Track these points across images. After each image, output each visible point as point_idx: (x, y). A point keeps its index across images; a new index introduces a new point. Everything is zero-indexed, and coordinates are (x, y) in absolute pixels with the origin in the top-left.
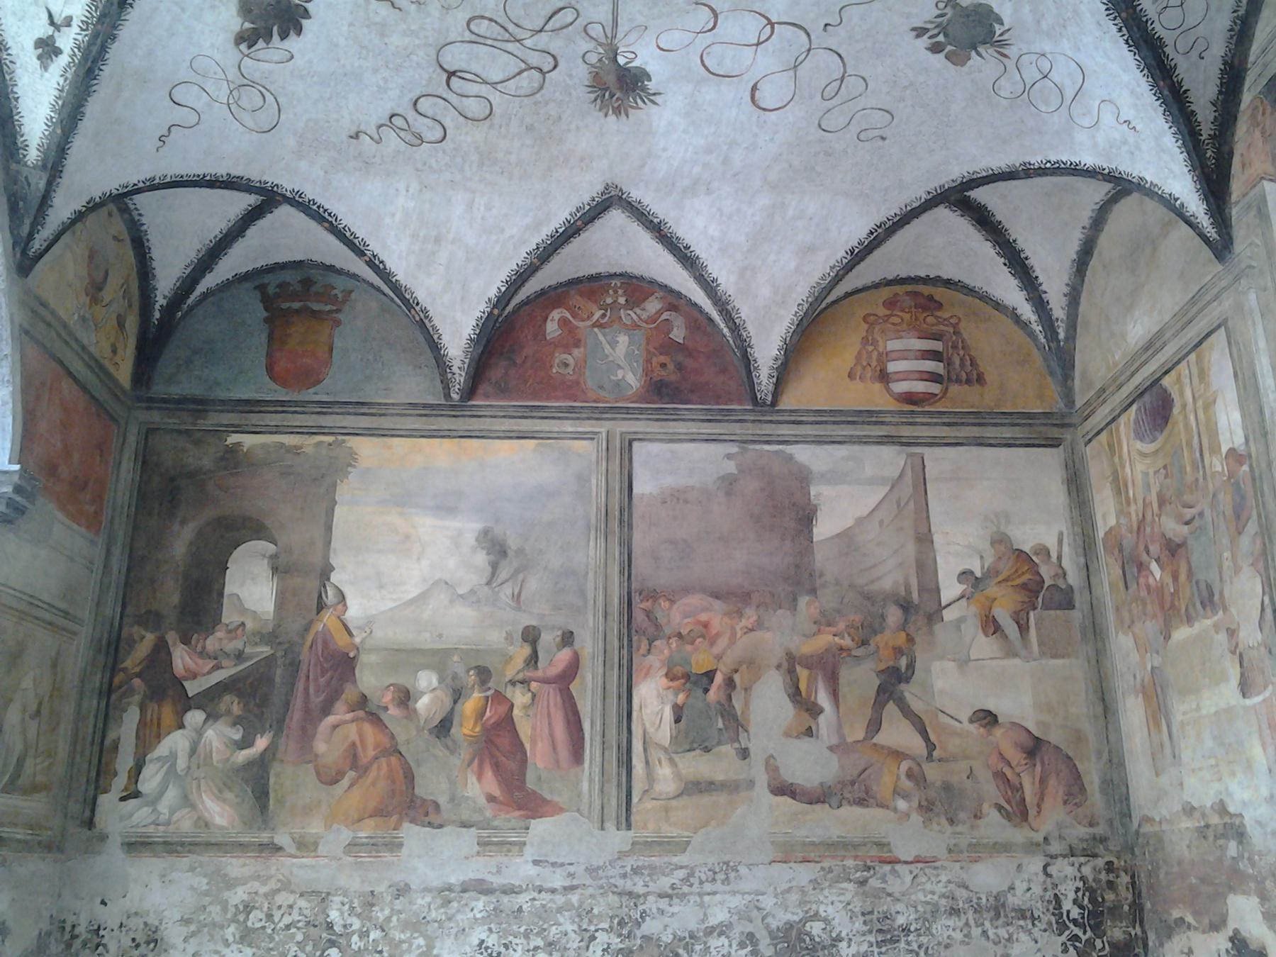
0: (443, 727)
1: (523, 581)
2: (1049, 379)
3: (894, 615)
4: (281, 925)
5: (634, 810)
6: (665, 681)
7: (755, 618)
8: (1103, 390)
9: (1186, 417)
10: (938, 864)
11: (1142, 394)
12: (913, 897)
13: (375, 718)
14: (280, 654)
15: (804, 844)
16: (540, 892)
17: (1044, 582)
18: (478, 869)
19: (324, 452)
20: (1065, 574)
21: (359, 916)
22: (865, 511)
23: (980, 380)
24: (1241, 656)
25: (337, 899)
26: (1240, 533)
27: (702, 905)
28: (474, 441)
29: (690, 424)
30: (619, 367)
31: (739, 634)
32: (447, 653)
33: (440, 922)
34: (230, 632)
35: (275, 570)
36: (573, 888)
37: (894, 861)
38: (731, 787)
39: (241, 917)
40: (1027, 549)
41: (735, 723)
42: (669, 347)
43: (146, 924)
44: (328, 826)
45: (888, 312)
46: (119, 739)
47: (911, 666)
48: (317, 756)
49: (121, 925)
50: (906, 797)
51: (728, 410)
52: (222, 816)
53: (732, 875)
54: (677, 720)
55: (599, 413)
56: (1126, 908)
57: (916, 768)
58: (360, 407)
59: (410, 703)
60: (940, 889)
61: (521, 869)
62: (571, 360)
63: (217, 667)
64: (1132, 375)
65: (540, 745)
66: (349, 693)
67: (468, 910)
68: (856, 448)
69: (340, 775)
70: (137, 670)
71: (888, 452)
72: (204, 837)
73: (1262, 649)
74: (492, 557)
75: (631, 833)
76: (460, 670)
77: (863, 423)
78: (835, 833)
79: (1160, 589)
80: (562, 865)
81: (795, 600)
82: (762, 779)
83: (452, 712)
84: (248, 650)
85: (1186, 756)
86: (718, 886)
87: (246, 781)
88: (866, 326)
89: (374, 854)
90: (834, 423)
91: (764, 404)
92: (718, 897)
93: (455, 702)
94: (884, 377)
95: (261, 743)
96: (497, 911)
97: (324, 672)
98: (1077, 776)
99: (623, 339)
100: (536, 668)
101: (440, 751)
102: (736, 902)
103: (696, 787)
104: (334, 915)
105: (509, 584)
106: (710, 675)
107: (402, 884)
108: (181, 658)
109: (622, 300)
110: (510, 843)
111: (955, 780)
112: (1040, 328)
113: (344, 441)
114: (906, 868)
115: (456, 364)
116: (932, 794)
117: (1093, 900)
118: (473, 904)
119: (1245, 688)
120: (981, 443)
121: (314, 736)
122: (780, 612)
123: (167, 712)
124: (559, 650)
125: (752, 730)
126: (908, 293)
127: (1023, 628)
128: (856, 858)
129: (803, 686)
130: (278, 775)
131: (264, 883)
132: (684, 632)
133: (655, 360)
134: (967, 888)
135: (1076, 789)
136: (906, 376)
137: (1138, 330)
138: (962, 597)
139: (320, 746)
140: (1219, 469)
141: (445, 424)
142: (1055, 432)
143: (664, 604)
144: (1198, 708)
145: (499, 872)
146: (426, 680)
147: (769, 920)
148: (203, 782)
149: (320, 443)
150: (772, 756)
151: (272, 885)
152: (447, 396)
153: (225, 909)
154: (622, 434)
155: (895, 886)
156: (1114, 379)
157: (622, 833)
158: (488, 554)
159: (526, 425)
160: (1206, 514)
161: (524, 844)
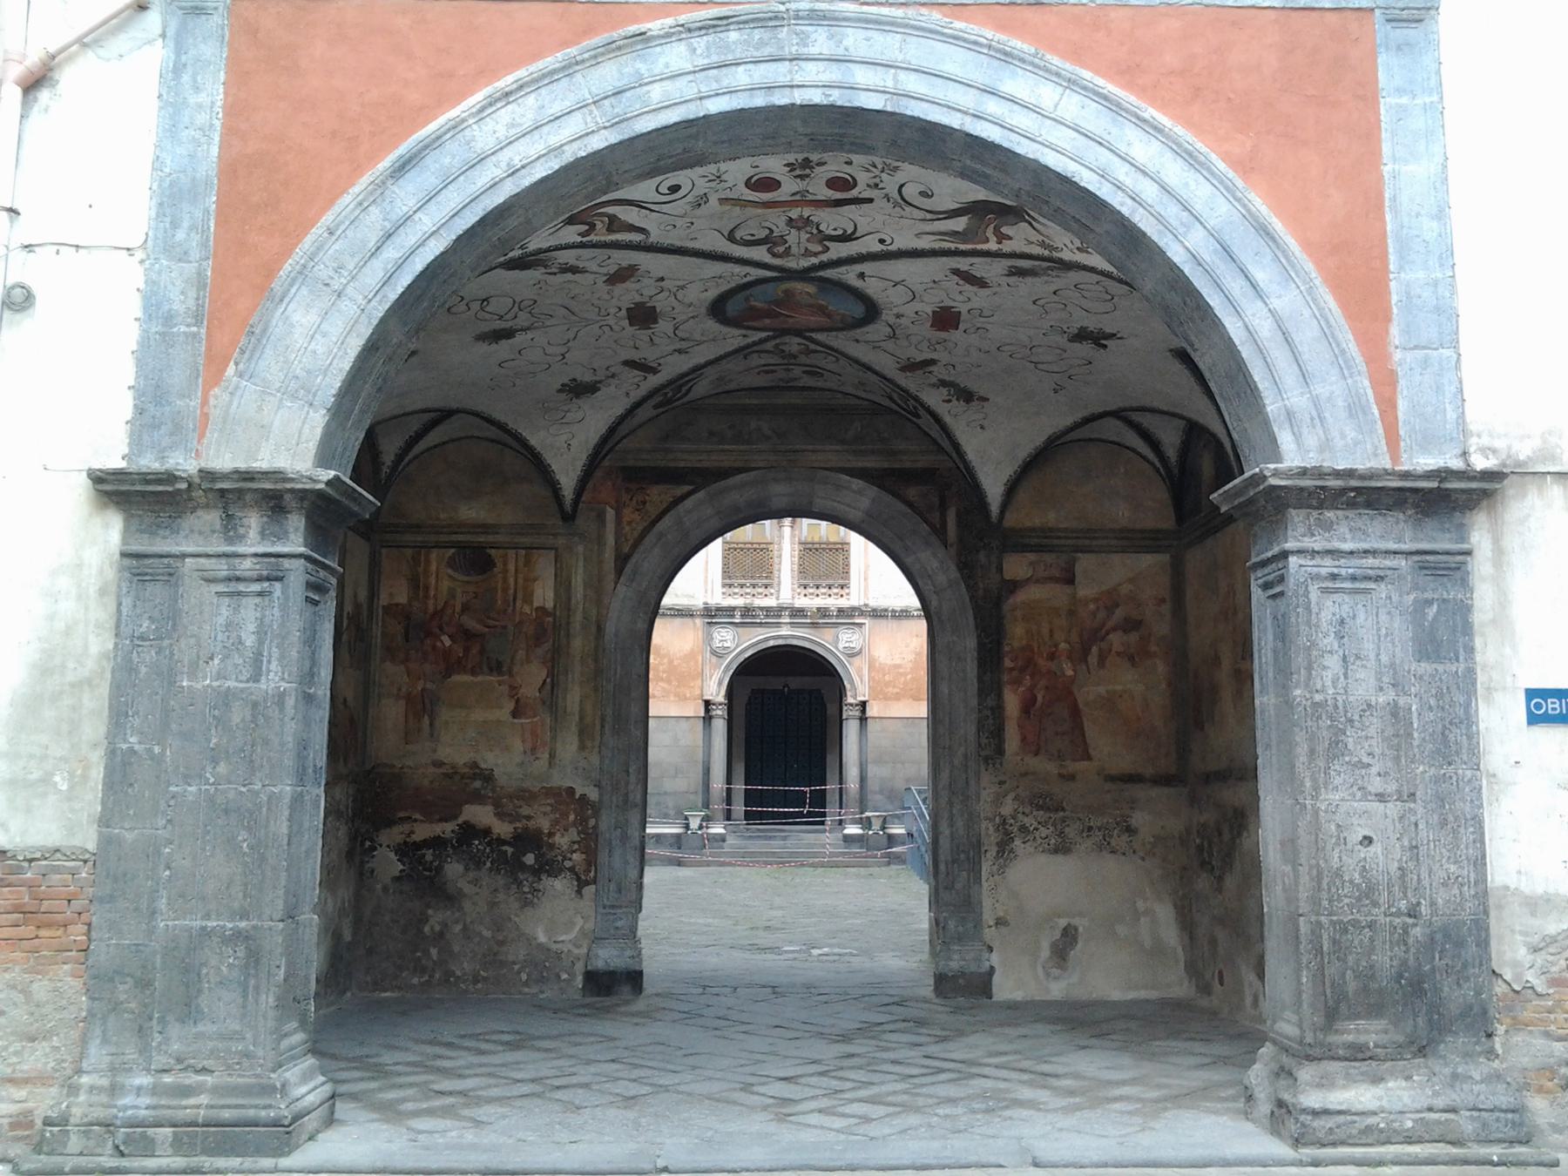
8: (418, 526)
79: (447, 653)
137: (470, 512)
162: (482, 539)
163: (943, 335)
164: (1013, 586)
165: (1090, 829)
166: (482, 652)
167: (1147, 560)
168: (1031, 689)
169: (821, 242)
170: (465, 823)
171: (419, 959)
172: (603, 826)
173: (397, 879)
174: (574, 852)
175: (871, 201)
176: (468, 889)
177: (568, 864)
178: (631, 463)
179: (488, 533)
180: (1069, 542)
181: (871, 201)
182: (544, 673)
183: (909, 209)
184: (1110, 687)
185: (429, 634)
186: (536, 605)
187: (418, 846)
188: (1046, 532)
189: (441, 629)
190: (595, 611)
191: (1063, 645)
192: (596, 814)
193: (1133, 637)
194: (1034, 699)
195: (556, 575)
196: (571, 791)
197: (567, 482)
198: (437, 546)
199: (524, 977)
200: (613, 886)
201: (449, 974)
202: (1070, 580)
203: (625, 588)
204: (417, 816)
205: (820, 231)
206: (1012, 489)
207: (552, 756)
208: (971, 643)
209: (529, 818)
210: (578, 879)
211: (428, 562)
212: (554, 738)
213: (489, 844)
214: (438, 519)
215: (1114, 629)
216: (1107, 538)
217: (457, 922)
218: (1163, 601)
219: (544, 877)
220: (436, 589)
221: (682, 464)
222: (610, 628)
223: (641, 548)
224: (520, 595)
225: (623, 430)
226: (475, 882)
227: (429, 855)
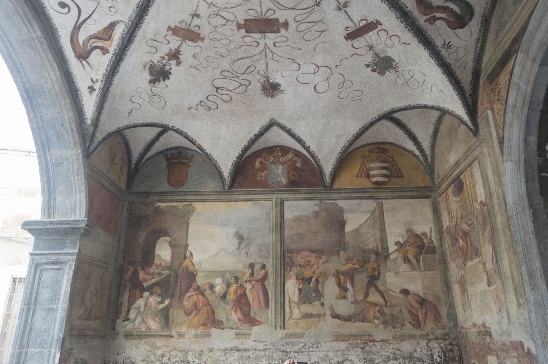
0: (224, 296)
1: (249, 248)
2: (426, 175)
3: (373, 257)
4: (173, 361)
5: (286, 323)
6: (295, 280)
7: (326, 259)
8: (443, 179)
9: (467, 190)
10: (389, 342)
11: (454, 181)
12: (381, 353)
13: (203, 294)
14: (172, 273)
15: (343, 335)
16: (256, 351)
17: (425, 245)
18: (236, 343)
19: (185, 207)
20: (432, 242)
21: (198, 358)
22: (363, 222)
23: (402, 176)
24: (487, 273)
25: (191, 353)
27: (309, 355)
28: (233, 202)
29: (303, 194)
30: (279, 176)
31: (320, 265)
32: (225, 272)
33: (223, 361)
34: (157, 266)
35: (171, 246)
36: (266, 349)
37: (374, 341)
38: (318, 316)
39: (161, 359)
40: (419, 233)
41: (319, 295)
42: (296, 169)
43: (131, 361)
44: (188, 329)
45: (369, 154)
46: (123, 301)
47: (379, 274)
48: (184, 306)
49: (123, 362)
50: (378, 319)
51: (316, 189)
52: (155, 326)
53: (319, 345)
54: (300, 293)
55: (273, 193)
56: (457, 359)
57: (381, 309)
58: (196, 193)
59: (213, 288)
60: (390, 351)
61: (249, 343)
62: (264, 175)
63: (153, 278)
65: (255, 302)
66: (194, 286)
67: (232, 356)
68: (359, 201)
69: (192, 312)
70: (128, 279)
71: (370, 202)
72: (149, 333)
74: (239, 240)
75: (285, 331)
76: (229, 277)
77: (362, 192)
78: (354, 331)
80: (263, 342)
81: (339, 253)
82: (329, 313)
83: (226, 291)
84: (162, 272)
85: (473, 306)
86: (314, 349)
87: (162, 315)
88: (362, 159)
89: (202, 338)
90: (352, 192)
91: (328, 187)
92: (314, 353)
93: (228, 288)
94: (368, 176)
95: (167, 302)
96: (242, 357)
97: (186, 279)
98: (438, 312)
99: (281, 167)
100: (253, 277)
101: (223, 304)
102: (320, 354)
103: (306, 316)
104: (190, 358)
105: (245, 249)
106: (311, 278)
107: (211, 348)
108: (142, 275)
109: (280, 154)
110: (246, 335)
111: (395, 313)
113: (192, 204)
114: (378, 343)
115: (227, 178)
116: (387, 318)
117: (445, 355)
118: (234, 354)
119: (489, 284)
120: (402, 197)
121: (183, 300)
122: (334, 257)
123: (138, 292)
124: (261, 270)
125: (325, 296)
126: (376, 148)
127: (418, 261)
128: (361, 340)
129: (342, 282)
130: (172, 312)
131: (168, 348)
132: (302, 264)
133: (291, 174)
134: (400, 350)
135: (437, 317)
136: (376, 176)
137: (452, 159)
138: (396, 250)
139: (185, 303)
140: (478, 208)
141: (224, 197)
142: (428, 193)
143: (295, 255)
144: (476, 290)
145: (242, 344)
146: (218, 281)
147: (332, 361)
148: (149, 315)
149: (184, 205)
150: (332, 305)
151: (170, 348)
152: (224, 188)
153: (155, 357)
154: (280, 198)
155: (374, 349)
156: (446, 175)
157: (282, 331)
158: (238, 239)
159: (249, 197)
161: (250, 335)
179: (458, 166)
186: (479, 201)
195: (482, 176)
214: (447, 170)
222: (510, 200)
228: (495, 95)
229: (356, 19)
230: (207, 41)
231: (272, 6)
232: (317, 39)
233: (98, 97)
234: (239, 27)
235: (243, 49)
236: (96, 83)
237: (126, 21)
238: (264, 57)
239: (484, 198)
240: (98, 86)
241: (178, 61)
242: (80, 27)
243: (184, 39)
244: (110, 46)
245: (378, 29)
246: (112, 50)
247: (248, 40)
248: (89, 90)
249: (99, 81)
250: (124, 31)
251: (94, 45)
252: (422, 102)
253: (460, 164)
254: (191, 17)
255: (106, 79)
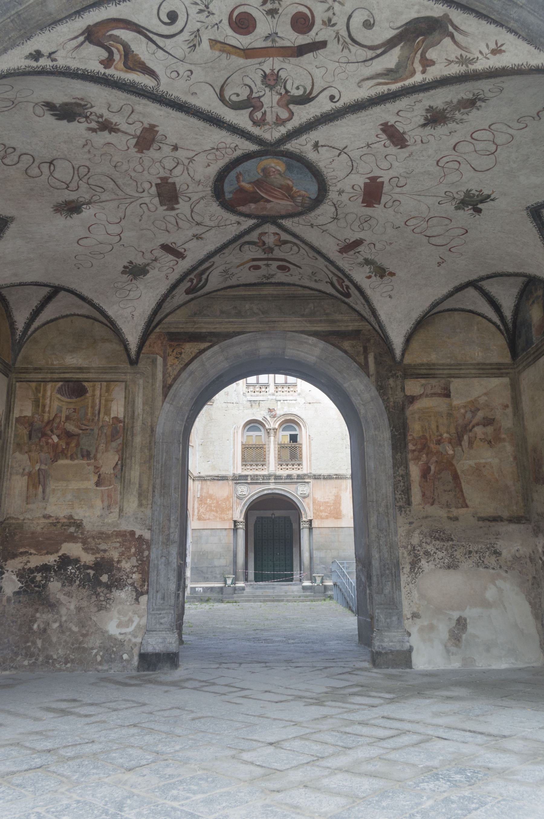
8: (40, 369)
26: (112, 441)
64: (64, 373)
73: (112, 475)
79: (55, 446)
85: (52, 500)
112: (21, 334)
119: (98, 484)
140: (108, 420)
144: (67, 486)
156: (49, 369)
160: (95, 430)
162: (80, 376)
163: (369, 211)
164: (412, 399)
165: (470, 552)
166: (78, 445)
167: (495, 382)
168: (427, 463)
169: (286, 106)
170: (63, 555)
171: (29, 647)
172: (153, 556)
173: (16, 593)
174: (134, 573)
175: (323, 44)
176: (63, 598)
177: (130, 581)
178: (173, 330)
179: (83, 373)
180: (445, 372)
181: (323, 44)
182: (117, 458)
183: (354, 48)
184: (477, 461)
185: (44, 435)
186: (112, 416)
187: (31, 571)
188: (430, 366)
189: (52, 431)
190: (150, 420)
191: (445, 435)
192: (149, 548)
193: (490, 429)
194: (429, 468)
195: (125, 398)
196: (132, 533)
197: (133, 340)
198: (52, 380)
199: (99, 658)
200: (159, 595)
201: (48, 657)
202: (447, 395)
203: (169, 405)
204: (32, 551)
205: (287, 92)
206: (408, 340)
207: (121, 510)
208: (387, 434)
209: (105, 551)
210: (137, 591)
211: (45, 390)
212: (122, 499)
213: (78, 569)
214: (54, 365)
215: (478, 424)
216: (468, 369)
217: (55, 622)
218: (507, 406)
219: (113, 590)
220: (50, 407)
221: (204, 330)
222: (159, 430)
223: (179, 381)
224: (102, 410)
225: (167, 307)
226: (69, 594)
227: (38, 577)
228: (173, 351)
229: (186, 246)
230: (139, 155)
231: (193, 199)
232: (156, 229)
233: (27, 69)
234: (164, 180)
235: (131, 182)
236: (49, 59)
237: (161, 88)
238: (121, 197)
239: (122, 416)
240: (44, 62)
241: (98, 130)
242: (139, 32)
243: (139, 137)
244: (116, 68)
245: (177, 259)
246: (110, 71)
247: (146, 186)
248: (35, 53)
249: (55, 63)
250: (146, 86)
251: (115, 50)
252: (105, 307)
253: (89, 372)
254: (174, 144)
255: (61, 72)
